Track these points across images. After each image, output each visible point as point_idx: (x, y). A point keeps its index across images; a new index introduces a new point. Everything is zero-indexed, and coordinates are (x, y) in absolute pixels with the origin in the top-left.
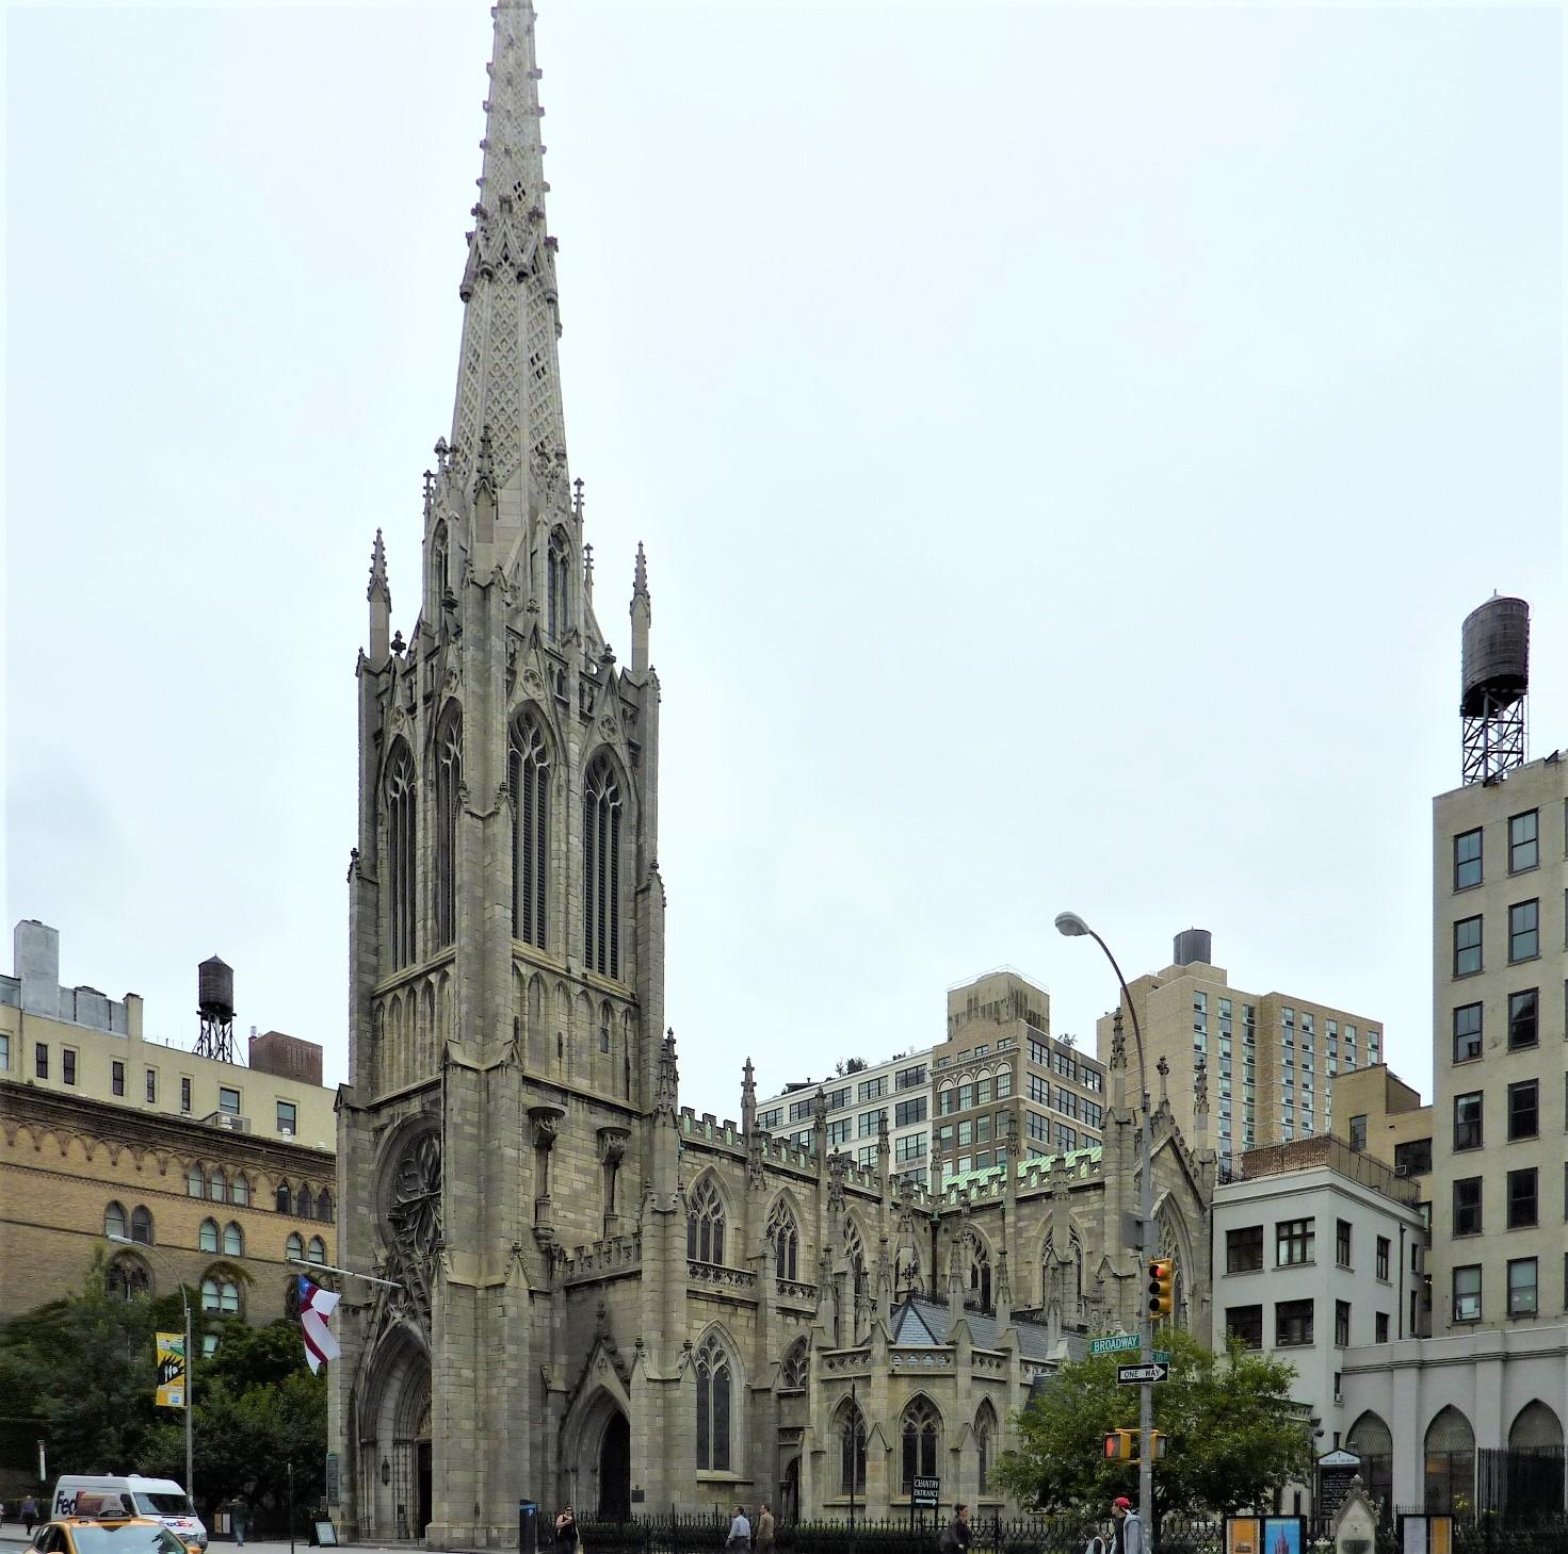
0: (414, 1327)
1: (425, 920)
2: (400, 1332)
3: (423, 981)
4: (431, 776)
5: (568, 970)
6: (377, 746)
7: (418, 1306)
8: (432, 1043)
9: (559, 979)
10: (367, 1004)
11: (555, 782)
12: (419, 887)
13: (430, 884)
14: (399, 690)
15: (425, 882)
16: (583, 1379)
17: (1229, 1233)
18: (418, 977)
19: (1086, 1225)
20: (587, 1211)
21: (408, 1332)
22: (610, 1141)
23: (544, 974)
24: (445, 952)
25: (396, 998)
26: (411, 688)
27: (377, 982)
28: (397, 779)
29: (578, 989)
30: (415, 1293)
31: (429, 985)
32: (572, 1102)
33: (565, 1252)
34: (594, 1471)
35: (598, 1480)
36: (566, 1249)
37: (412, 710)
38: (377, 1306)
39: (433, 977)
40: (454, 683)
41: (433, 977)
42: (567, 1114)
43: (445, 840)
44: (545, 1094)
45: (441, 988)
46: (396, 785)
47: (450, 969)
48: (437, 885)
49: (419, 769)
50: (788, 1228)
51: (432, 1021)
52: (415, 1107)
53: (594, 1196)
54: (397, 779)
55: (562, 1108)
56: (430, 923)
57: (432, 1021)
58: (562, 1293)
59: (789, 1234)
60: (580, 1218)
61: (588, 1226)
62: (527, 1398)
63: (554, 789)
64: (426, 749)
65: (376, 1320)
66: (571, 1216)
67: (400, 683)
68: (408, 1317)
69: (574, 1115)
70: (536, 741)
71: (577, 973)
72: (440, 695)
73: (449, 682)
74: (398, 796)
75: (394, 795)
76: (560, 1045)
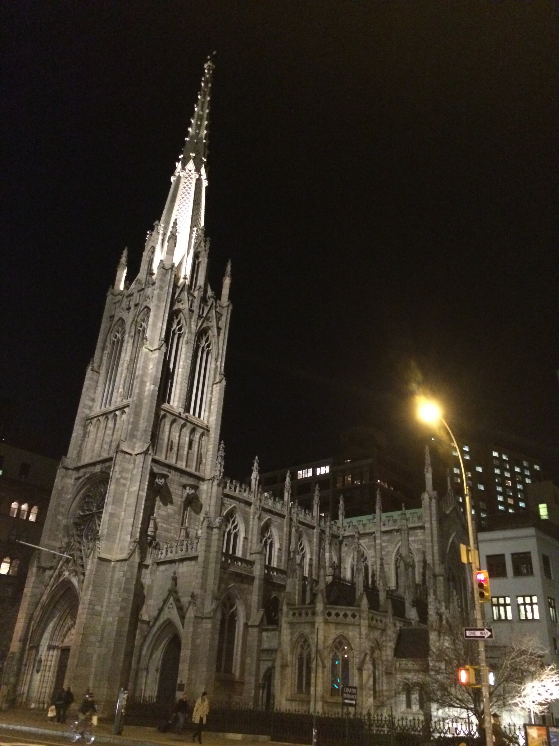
0: (75, 581)
1: (119, 389)
2: (67, 584)
3: (113, 414)
4: (133, 334)
5: (180, 414)
6: (110, 321)
7: (80, 569)
8: (111, 441)
9: (174, 417)
10: (84, 422)
11: (185, 339)
12: (118, 376)
13: (124, 375)
14: (124, 302)
15: (122, 374)
16: (159, 614)
17: (488, 557)
18: (111, 412)
19: (416, 547)
20: (173, 524)
21: (71, 583)
22: (188, 491)
23: (168, 414)
24: (125, 402)
25: (99, 420)
26: (130, 302)
27: (91, 412)
28: (117, 334)
29: (183, 422)
30: (79, 561)
31: (116, 415)
32: (173, 472)
33: (159, 544)
34: (157, 670)
35: (158, 677)
36: (160, 543)
37: (129, 309)
38: (56, 569)
39: (118, 413)
40: (148, 300)
41: (118, 413)
42: (170, 477)
43: (133, 359)
44: (161, 468)
45: (121, 417)
46: (116, 336)
47: (126, 410)
48: (126, 376)
49: (127, 331)
50: (269, 538)
51: (114, 431)
52: (98, 469)
53: (177, 517)
54: (117, 334)
55: (168, 474)
56: (121, 390)
57: (114, 431)
58: (155, 565)
59: (269, 541)
60: (169, 527)
61: (173, 531)
62: (127, 625)
63: (184, 342)
64: (132, 323)
65: (54, 576)
66: (165, 526)
67: (125, 298)
68: (72, 575)
69: (173, 478)
70: (178, 323)
71: (183, 416)
72: (141, 305)
73: (146, 300)
74: (116, 340)
75: (114, 339)
76: (172, 446)
